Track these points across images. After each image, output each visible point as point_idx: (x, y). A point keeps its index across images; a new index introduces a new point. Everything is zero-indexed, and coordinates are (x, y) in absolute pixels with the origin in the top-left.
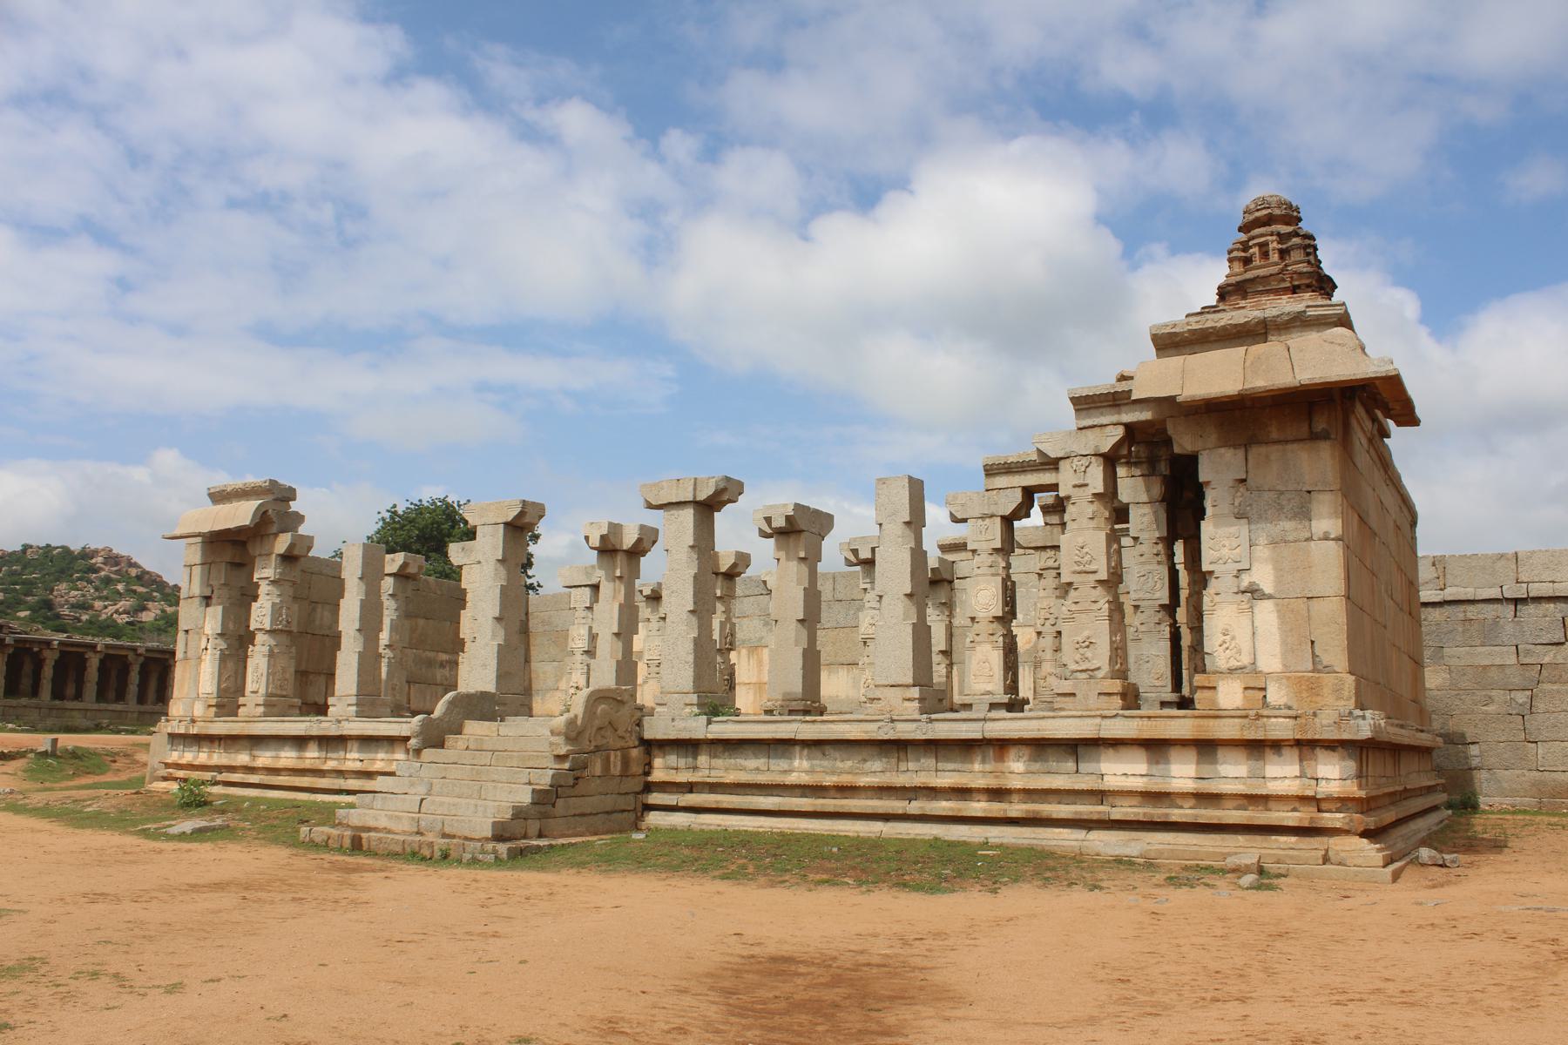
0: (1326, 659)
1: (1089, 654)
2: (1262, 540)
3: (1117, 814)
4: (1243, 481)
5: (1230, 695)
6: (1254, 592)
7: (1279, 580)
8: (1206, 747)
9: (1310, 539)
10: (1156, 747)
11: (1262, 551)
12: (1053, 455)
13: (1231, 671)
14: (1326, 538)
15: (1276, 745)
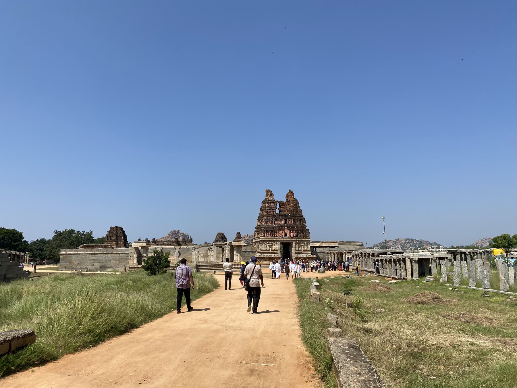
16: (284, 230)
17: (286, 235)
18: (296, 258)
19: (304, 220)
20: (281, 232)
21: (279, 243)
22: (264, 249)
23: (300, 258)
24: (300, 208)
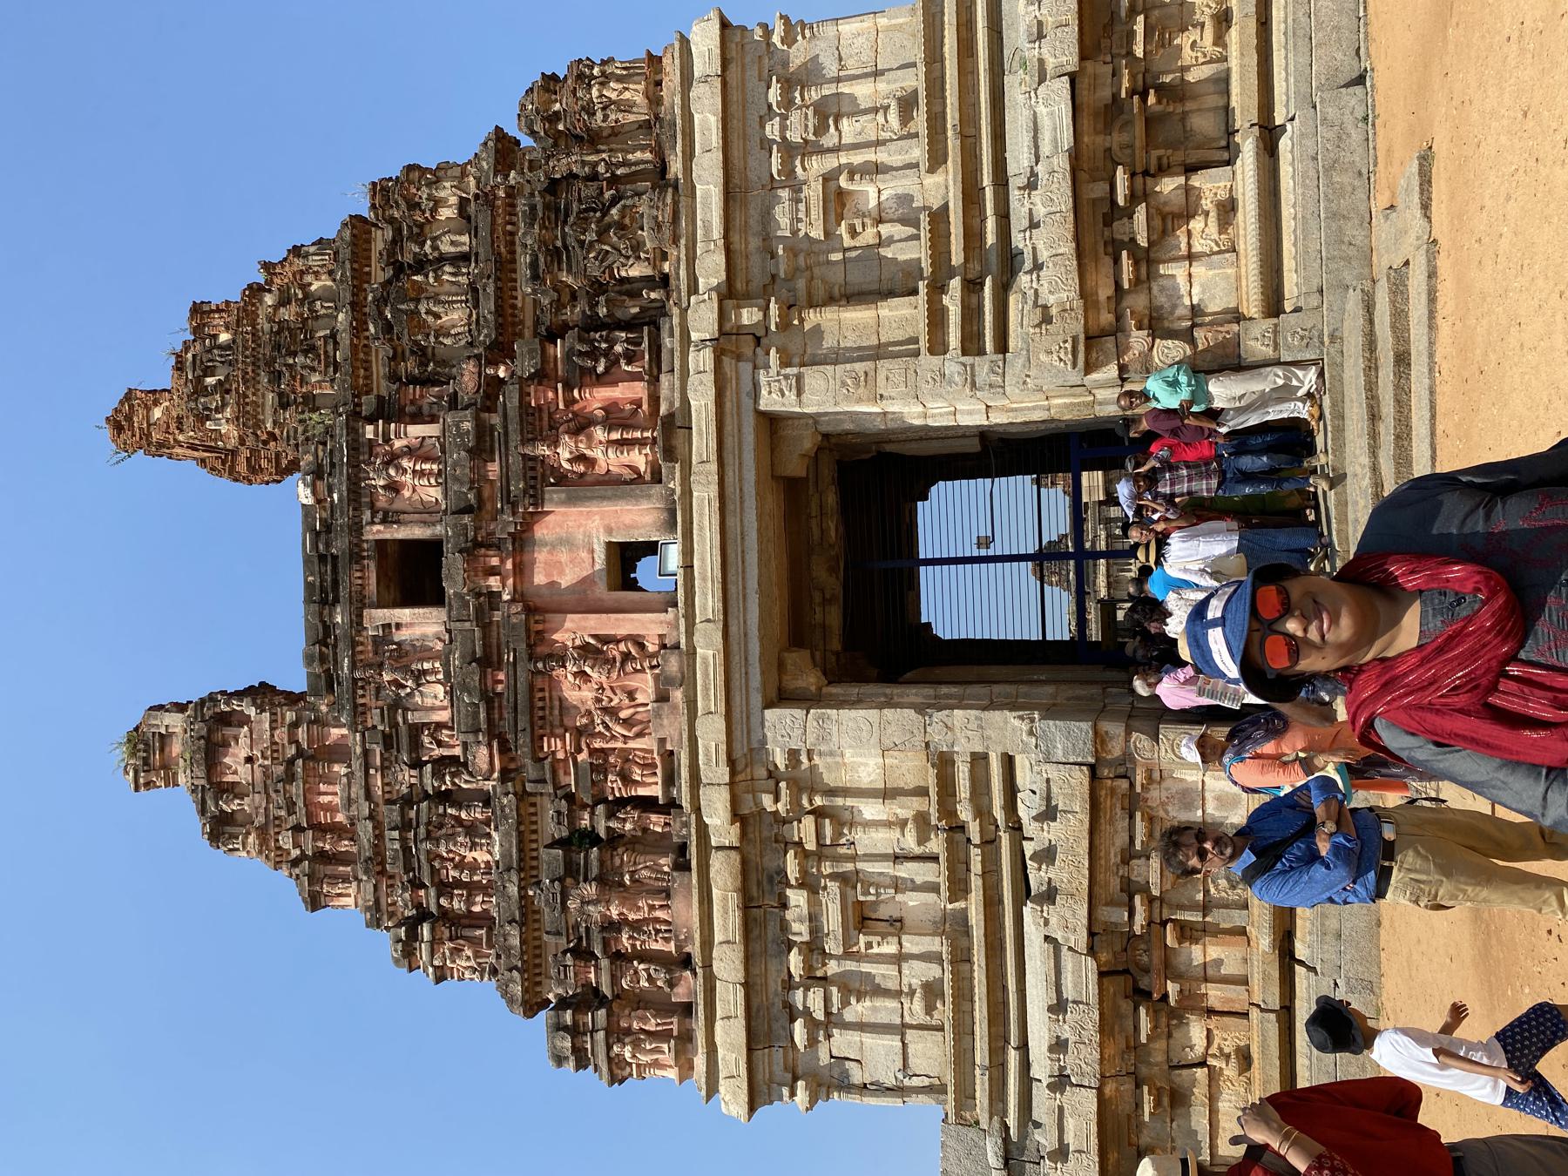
16: (539, 610)
18: (1096, 343)
19: (401, 196)
20: (577, 691)
21: (784, 729)
22: (931, 1055)
23: (1095, 226)
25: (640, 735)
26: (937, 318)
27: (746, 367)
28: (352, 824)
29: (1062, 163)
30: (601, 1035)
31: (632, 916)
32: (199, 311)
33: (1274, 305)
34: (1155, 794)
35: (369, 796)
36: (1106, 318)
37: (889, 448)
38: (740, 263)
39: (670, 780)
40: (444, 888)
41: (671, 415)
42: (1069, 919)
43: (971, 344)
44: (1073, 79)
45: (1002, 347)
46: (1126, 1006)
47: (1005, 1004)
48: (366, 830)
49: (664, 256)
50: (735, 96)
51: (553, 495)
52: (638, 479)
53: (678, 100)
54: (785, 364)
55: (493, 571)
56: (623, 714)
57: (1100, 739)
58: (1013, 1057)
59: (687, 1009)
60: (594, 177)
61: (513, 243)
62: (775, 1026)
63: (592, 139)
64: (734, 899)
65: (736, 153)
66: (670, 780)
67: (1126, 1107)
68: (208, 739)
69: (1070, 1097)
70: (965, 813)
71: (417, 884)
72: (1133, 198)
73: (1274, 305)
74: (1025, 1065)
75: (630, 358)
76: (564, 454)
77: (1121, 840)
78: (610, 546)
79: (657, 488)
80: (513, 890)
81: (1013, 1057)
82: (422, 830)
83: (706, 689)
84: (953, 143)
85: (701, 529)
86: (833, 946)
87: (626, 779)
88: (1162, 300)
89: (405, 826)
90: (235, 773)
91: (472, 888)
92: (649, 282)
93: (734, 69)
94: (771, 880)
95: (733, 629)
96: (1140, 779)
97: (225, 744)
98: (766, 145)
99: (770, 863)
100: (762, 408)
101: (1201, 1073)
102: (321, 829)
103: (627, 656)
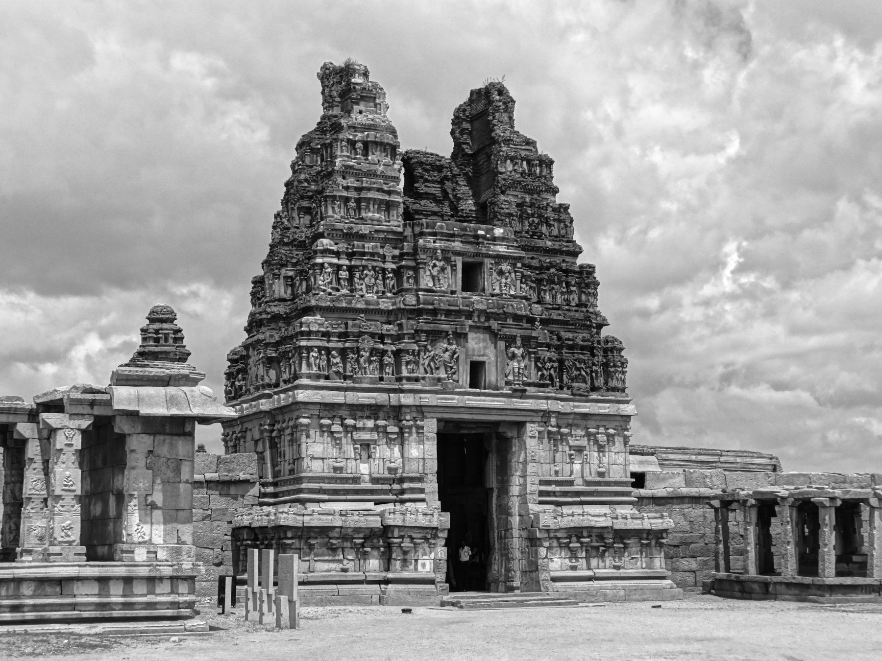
0: (183, 538)
1: (69, 533)
2: (159, 481)
3: (86, 614)
4: (151, 452)
5: (140, 555)
6: (153, 506)
7: (164, 501)
8: (128, 581)
9: (180, 482)
10: (103, 581)
11: (158, 487)
12: (55, 426)
13: (140, 543)
14: (187, 482)
15: (161, 579)
17: (477, 369)
24: (559, 199)
25: (425, 369)
26: (548, 483)
27: (539, 419)
28: (362, 219)
29: (593, 524)
30: (320, 344)
31: (362, 360)
32: (547, 163)
33: (554, 579)
34: (426, 545)
35: (377, 231)
36: (552, 535)
37: (490, 455)
38: (567, 417)
39: (409, 379)
40: (351, 269)
41: (525, 391)
42: (394, 520)
43: (542, 493)
44: (612, 527)
45: (541, 503)
46: (361, 535)
47: (339, 495)
48: (365, 229)
49: (568, 389)
50: (612, 418)
51: (502, 344)
52: (506, 376)
53: (613, 398)
54: (540, 432)
55: (479, 317)
56: (432, 364)
57: (443, 530)
58: (326, 497)
59: (327, 378)
60: (594, 364)
61: (572, 325)
62: (326, 412)
63: (606, 365)
64: (373, 401)
65: (597, 417)
66: (409, 379)
67: (331, 534)
68: (388, 144)
69: (337, 517)
70: (406, 485)
71: (350, 256)
72: (581, 543)
73: (554, 579)
74: (324, 501)
75: (543, 375)
76: (516, 351)
77: (414, 535)
78: (483, 363)
79: (503, 383)
80: (359, 306)
81: (326, 497)
82: (375, 264)
83: (445, 399)
84: (592, 488)
85: (494, 401)
86: (356, 436)
87: (408, 363)
88: (555, 550)
89: (372, 254)
90: (373, 154)
91: (350, 280)
92: (561, 381)
93: (620, 418)
94: (376, 414)
95: (462, 410)
96: (433, 541)
97: (385, 150)
98: (598, 427)
99: (381, 414)
100: (528, 425)
101: (341, 557)
102: (358, 201)
103: (452, 368)
